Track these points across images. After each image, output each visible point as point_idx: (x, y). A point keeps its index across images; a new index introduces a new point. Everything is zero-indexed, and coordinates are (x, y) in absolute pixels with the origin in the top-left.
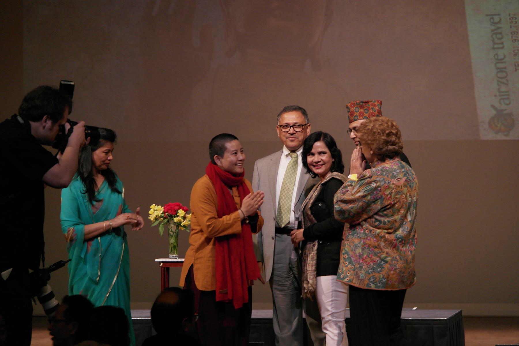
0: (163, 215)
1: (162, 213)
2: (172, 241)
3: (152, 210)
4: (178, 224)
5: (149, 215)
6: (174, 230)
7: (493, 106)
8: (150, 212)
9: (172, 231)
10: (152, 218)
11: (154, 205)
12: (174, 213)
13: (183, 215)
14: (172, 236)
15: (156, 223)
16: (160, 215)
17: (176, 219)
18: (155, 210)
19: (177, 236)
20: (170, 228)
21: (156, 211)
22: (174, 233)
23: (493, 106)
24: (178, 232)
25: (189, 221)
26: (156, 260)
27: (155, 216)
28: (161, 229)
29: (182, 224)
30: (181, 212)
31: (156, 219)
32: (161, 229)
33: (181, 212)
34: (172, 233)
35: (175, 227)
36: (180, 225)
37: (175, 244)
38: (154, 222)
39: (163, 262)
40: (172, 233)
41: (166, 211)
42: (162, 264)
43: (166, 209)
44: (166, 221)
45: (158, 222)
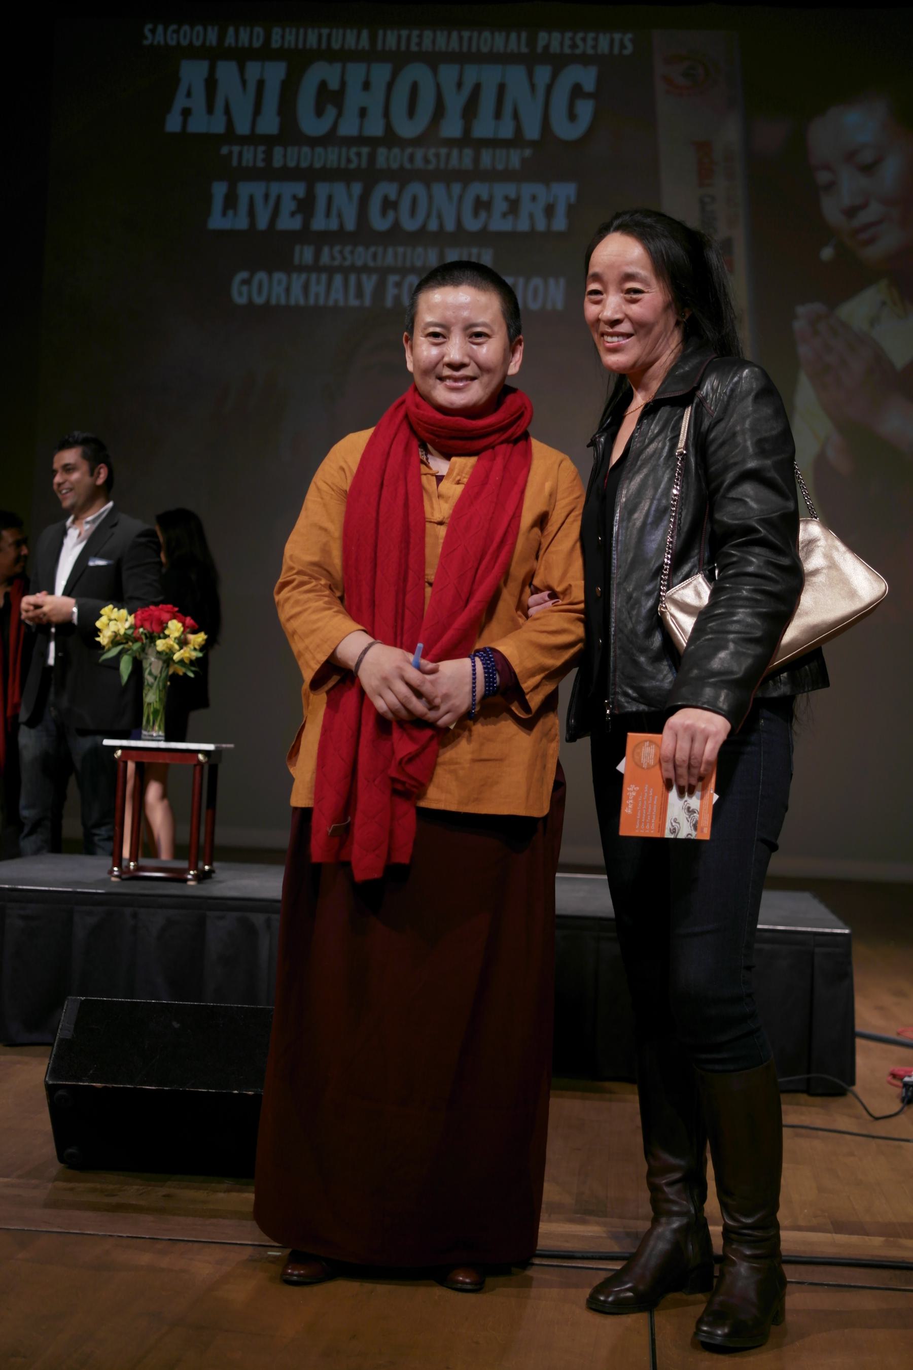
0: (130, 632)
1: (130, 628)
3: (104, 619)
4: (167, 658)
5: (97, 632)
6: (156, 670)
8: (98, 624)
9: (150, 673)
10: (104, 639)
11: (111, 606)
12: (156, 628)
13: (177, 634)
14: (151, 686)
16: (122, 632)
17: (161, 644)
18: (110, 620)
20: (145, 665)
22: (155, 678)
25: (195, 649)
28: (125, 668)
29: (176, 657)
30: (175, 627)
31: (116, 640)
32: (125, 668)
33: (175, 627)
34: (149, 679)
35: (160, 663)
36: (172, 659)
38: (109, 650)
39: (122, 748)
41: (139, 623)
43: (139, 617)
45: (120, 648)
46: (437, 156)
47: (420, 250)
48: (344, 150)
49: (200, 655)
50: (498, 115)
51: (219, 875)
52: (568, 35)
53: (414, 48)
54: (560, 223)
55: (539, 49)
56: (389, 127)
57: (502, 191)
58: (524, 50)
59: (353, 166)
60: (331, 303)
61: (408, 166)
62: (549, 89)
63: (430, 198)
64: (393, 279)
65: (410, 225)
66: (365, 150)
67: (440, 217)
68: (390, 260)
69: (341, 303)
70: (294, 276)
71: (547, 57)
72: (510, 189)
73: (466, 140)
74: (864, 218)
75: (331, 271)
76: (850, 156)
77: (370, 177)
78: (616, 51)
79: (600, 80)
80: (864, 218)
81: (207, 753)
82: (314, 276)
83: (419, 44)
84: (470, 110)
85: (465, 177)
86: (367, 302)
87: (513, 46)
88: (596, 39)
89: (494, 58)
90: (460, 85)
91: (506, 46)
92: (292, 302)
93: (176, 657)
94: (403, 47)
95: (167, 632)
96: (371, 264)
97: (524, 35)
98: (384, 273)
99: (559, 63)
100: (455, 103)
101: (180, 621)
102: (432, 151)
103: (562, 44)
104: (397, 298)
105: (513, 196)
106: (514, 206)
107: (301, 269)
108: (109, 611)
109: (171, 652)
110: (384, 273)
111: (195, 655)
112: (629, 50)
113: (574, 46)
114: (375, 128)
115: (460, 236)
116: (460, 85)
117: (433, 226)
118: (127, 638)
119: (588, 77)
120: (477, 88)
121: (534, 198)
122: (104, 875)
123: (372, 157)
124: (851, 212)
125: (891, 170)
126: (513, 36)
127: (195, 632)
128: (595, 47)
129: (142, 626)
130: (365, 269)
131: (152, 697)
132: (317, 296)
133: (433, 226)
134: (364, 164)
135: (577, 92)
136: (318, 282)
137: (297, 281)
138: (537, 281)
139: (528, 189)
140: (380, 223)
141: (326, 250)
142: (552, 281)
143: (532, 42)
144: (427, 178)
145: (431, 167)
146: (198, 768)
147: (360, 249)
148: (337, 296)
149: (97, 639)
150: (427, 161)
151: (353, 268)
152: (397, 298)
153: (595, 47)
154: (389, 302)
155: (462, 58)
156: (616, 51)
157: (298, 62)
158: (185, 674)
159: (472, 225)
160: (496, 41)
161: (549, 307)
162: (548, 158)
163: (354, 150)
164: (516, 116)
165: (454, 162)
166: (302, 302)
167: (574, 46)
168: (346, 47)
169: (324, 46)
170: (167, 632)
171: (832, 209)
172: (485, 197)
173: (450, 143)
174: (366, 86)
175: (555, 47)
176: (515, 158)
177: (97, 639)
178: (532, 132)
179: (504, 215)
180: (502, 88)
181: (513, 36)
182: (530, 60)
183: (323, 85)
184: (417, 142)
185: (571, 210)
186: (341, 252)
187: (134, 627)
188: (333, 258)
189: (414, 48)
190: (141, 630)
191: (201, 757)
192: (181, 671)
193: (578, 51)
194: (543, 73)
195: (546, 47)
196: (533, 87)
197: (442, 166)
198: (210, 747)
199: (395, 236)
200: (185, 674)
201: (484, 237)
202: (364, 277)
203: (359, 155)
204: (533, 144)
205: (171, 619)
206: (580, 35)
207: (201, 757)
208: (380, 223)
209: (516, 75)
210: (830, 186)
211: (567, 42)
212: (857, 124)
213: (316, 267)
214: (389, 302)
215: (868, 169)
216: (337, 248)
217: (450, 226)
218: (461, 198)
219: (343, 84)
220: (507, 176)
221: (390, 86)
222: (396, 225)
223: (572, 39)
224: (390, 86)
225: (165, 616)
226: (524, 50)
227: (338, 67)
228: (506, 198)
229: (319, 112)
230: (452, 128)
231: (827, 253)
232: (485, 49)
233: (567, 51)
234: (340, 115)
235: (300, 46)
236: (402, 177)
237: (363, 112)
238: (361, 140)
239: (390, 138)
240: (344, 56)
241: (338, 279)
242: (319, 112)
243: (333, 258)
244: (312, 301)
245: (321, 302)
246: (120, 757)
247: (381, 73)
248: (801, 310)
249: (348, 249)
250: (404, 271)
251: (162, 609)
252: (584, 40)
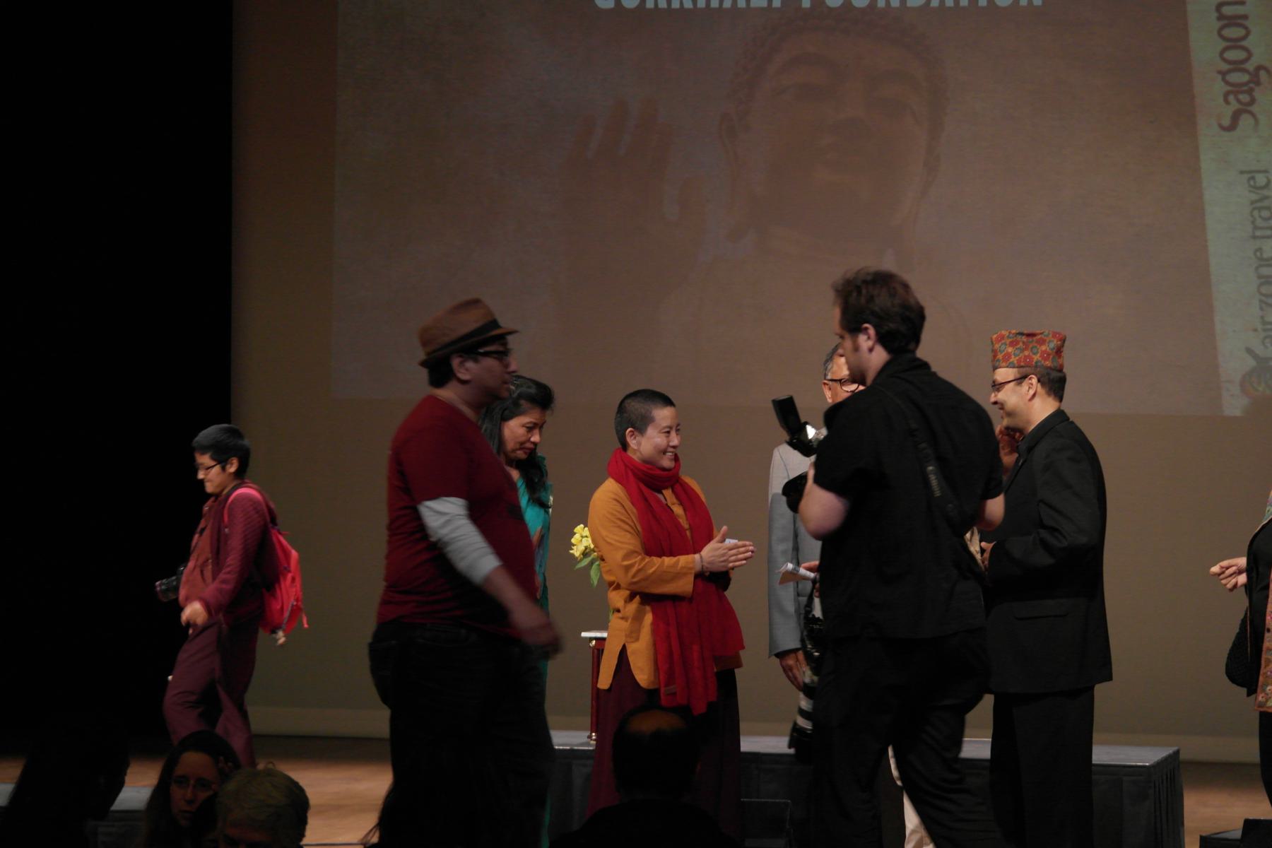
3: (577, 536)
5: (571, 545)
7: (1249, 351)
10: (577, 551)
15: (586, 562)
23: (1249, 351)
26: (584, 634)
27: (582, 548)
31: (585, 554)
39: (596, 639)
122: (586, 740)
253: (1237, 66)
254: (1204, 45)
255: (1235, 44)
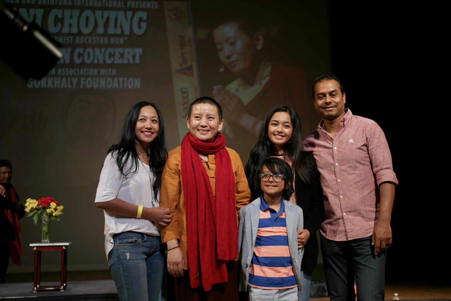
0: (37, 207)
2: (45, 228)
4: (50, 215)
5: (24, 207)
6: (46, 220)
8: (26, 205)
9: (44, 221)
10: (27, 210)
11: (30, 199)
13: (54, 207)
14: (44, 225)
15: (32, 214)
16: (34, 207)
17: (48, 211)
18: (30, 203)
19: (49, 225)
20: (42, 217)
21: (31, 204)
22: (46, 222)
24: (50, 222)
26: (31, 245)
27: (30, 208)
28: (35, 219)
29: (54, 214)
30: (53, 205)
31: (32, 210)
32: (35, 219)
33: (53, 205)
34: (44, 222)
36: (52, 216)
37: (46, 231)
38: (30, 213)
39: (36, 247)
40: (44, 222)
41: (40, 204)
42: (35, 248)
43: (40, 202)
44: (40, 212)
46: (96, 39)
47: (91, 69)
48: (64, 38)
49: (62, 213)
50: (116, 26)
51: (69, 287)
52: (137, 2)
53: (87, 5)
54: (137, 61)
55: (128, 6)
56: (79, 30)
57: (118, 51)
58: (123, 6)
59: (68, 42)
60: (62, 87)
61: (86, 42)
62: (132, 19)
63: (94, 53)
64: (83, 79)
65: (88, 61)
66: (72, 38)
67: (98, 58)
68: (81, 72)
69: (66, 87)
70: (49, 78)
71: (130, 9)
72: (121, 50)
73: (105, 34)
74: (232, 59)
75: (62, 77)
76: (227, 40)
77: (74, 46)
78: (153, 7)
79: (148, 16)
80: (232, 59)
81: (66, 246)
82: (56, 79)
83: (89, 4)
84: (106, 25)
85: (106, 46)
86: (74, 86)
87: (119, 5)
88: (146, 3)
89: (113, 9)
90: (102, 17)
91: (117, 4)
92: (49, 86)
93: (54, 214)
94: (83, 5)
95: (50, 206)
96: (75, 74)
97: (123, 2)
98: (80, 77)
99: (135, 11)
100: (101, 23)
101: (55, 202)
102: (94, 38)
103: (135, 5)
104: (85, 85)
105: (122, 52)
106: (122, 56)
107: (51, 76)
108: (29, 200)
109: (52, 213)
110: (80, 77)
111: (60, 213)
112: (156, 7)
113: (139, 5)
114: (75, 30)
115: (105, 65)
116: (102, 17)
117: (96, 62)
118: (38, 209)
119: (144, 15)
120: (108, 18)
121: (128, 53)
122: (31, 290)
123: (74, 40)
124: (228, 57)
125: (239, 44)
126: (119, 2)
127: (59, 206)
128: (146, 6)
129: (41, 205)
130: (73, 76)
131: (45, 228)
132: (57, 85)
133: (96, 62)
134: (71, 42)
135: (141, 20)
136: (57, 80)
137: (50, 80)
138: (131, 79)
139: (126, 50)
140: (78, 61)
141: (59, 70)
142: (136, 79)
143: (125, 4)
144: (93, 46)
145: (95, 42)
146: (63, 252)
147: (71, 69)
148: (64, 84)
149: (25, 210)
150: (92, 41)
151: (69, 75)
152: (85, 85)
153: (146, 6)
154: (82, 87)
155: (103, 9)
156: (153, 7)
157: (47, 9)
158: (56, 220)
159: (109, 61)
160: (115, 4)
161: (135, 87)
162: (132, 40)
163: (68, 38)
164: (121, 27)
165: (102, 41)
166: (52, 87)
167: (139, 5)
168: (64, 4)
169: (56, 4)
170: (50, 206)
171: (222, 56)
172: (112, 52)
173: (100, 35)
174: (71, 17)
175: (133, 6)
176: (122, 40)
177: (25, 210)
178: (127, 32)
179: (119, 58)
180: (116, 18)
181: (119, 2)
182: (125, 10)
183: (56, 17)
184: (89, 35)
185: (141, 57)
186: (65, 70)
187: (38, 205)
188: (62, 72)
189: (87, 5)
190: (41, 206)
191: (64, 248)
192: (53, 219)
193: (141, 7)
194: (130, 14)
195: (130, 6)
196: (126, 18)
197: (98, 42)
198: (67, 244)
199: (83, 65)
200: (56, 220)
201: (112, 65)
202: (73, 79)
203: (70, 39)
204: (127, 36)
205: (52, 201)
206: (141, 2)
207: (64, 248)
208: (78, 61)
209: (121, 14)
210: (221, 49)
211: (137, 5)
212: (228, 31)
213: (56, 75)
214: (82, 87)
215: (233, 44)
216: (63, 69)
217: (101, 62)
218: (104, 53)
219: (63, 16)
220: (119, 46)
221: (79, 17)
222: (83, 61)
223: (138, 3)
224: (79, 17)
225: (49, 201)
226: (123, 6)
227: (61, 11)
228: (120, 53)
229: (55, 25)
230: (101, 30)
231: (222, 70)
232: (110, 6)
233: (137, 7)
234: (63, 25)
235: (48, 3)
236: (85, 46)
237: (70, 25)
238: (70, 34)
239: (80, 34)
240: (63, 7)
241: (64, 79)
242: (55, 25)
243: (62, 72)
244: (55, 86)
245: (59, 86)
246: (36, 250)
247: (76, 13)
248: (215, 87)
249: (67, 69)
250: (87, 76)
251: (48, 199)
252: (142, 3)
253: (186, 103)
254: (178, 98)
255: (185, 98)
